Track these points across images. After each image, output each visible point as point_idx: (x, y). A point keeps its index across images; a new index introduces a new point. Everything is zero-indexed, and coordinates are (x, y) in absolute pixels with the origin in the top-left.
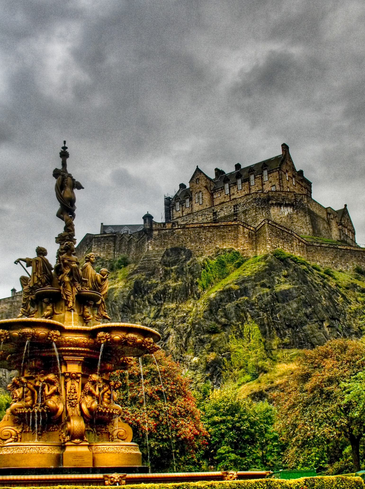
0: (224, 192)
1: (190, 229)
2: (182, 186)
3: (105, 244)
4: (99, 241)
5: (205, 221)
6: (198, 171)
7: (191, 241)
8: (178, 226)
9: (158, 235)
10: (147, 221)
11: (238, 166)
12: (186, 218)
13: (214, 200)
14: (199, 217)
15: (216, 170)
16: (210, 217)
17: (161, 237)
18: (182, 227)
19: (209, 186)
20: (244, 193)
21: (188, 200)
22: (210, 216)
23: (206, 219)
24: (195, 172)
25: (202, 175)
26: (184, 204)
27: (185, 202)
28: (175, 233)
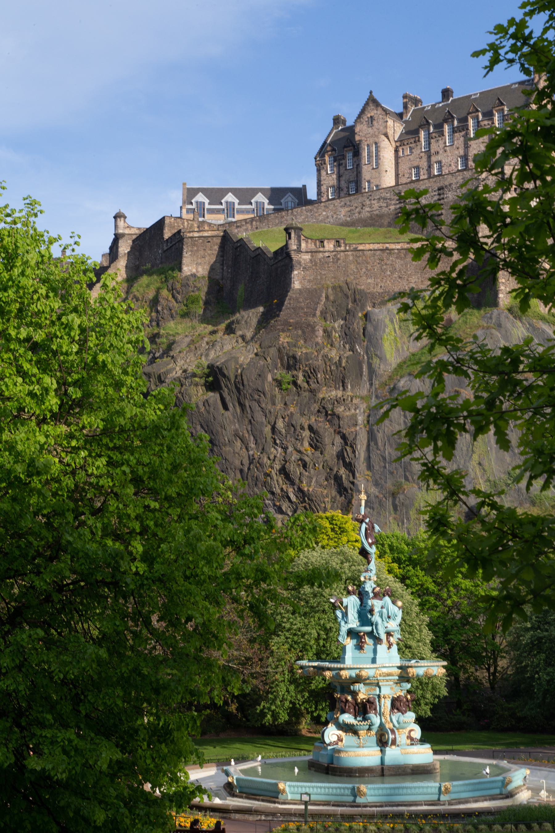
0: (419, 147)
1: (365, 252)
2: (337, 120)
3: (204, 250)
4: (195, 245)
5: (385, 210)
6: (372, 101)
7: (368, 277)
8: (345, 247)
9: (311, 260)
10: (293, 235)
11: (446, 93)
12: (350, 201)
13: (400, 161)
14: (373, 202)
15: (405, 97)
16: (395, 204)
17: (316, 265)
18: (352, 248)
19: (390, 132)
20: (457, 152)
21: (349, 155)
22: (393, 202)
23: (387, 207)
24: (367, 104)
25: (380, 111)
26: (343, 161)
27: (344, 157)
28: (338, 259)
